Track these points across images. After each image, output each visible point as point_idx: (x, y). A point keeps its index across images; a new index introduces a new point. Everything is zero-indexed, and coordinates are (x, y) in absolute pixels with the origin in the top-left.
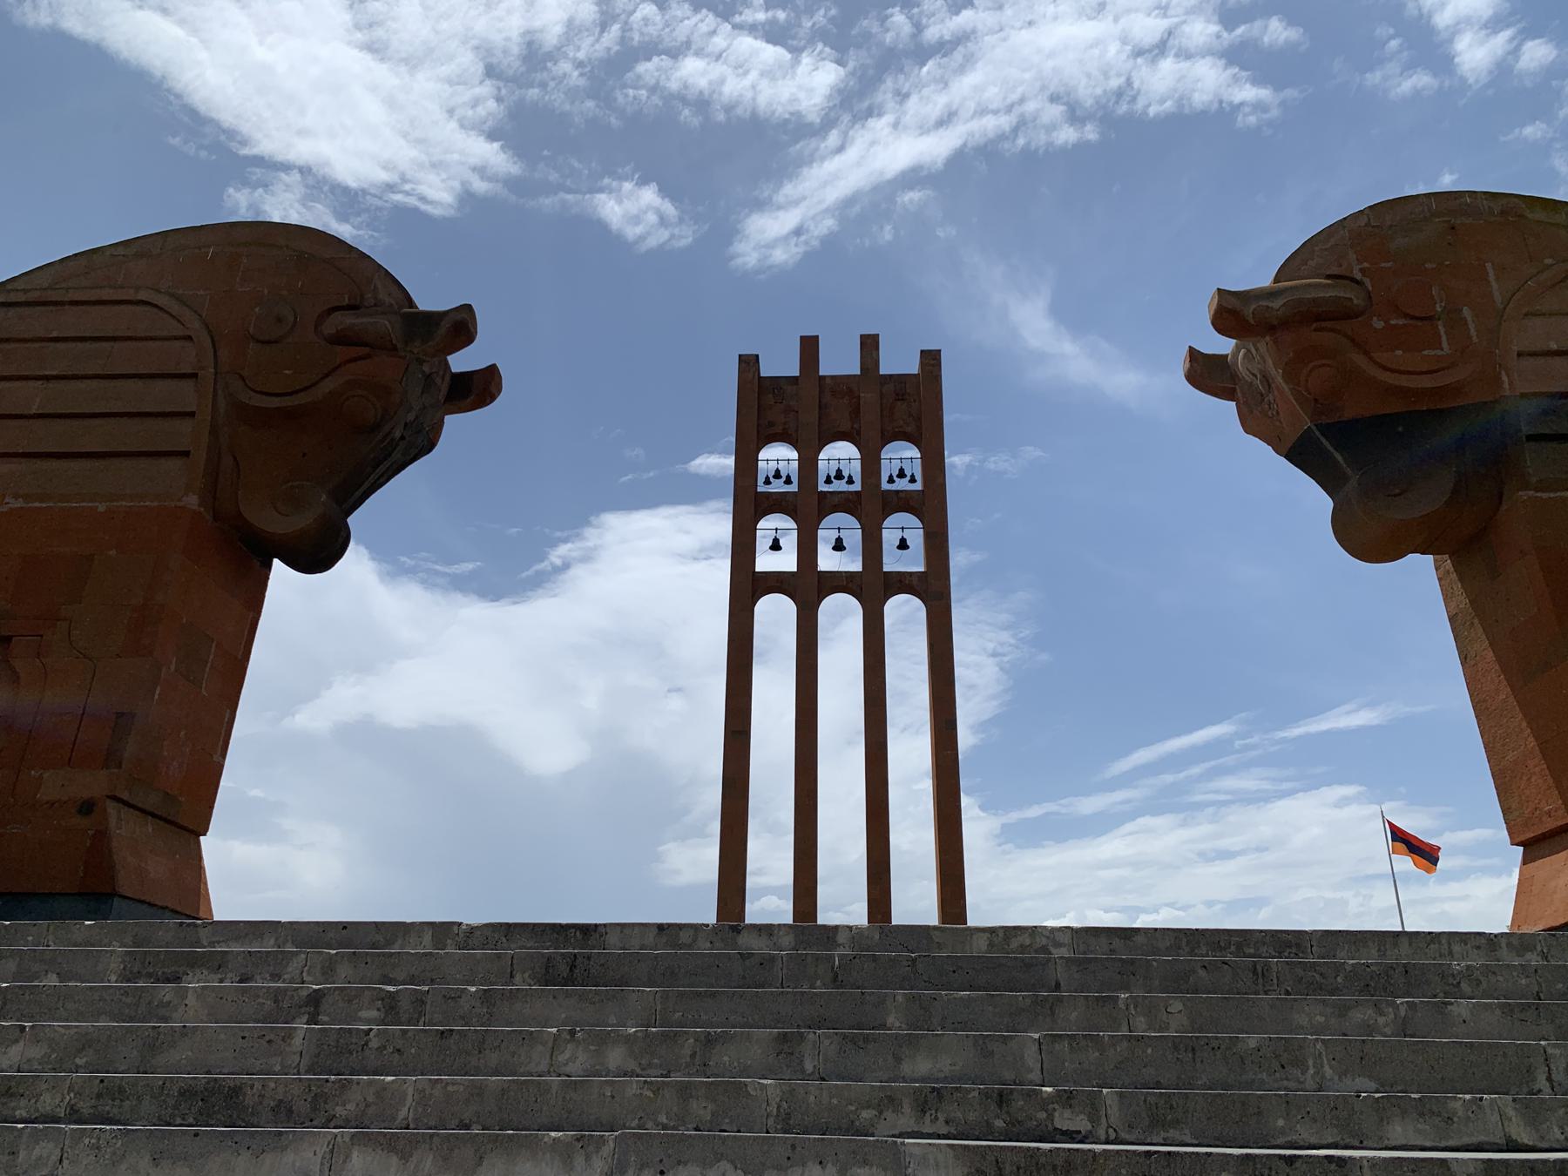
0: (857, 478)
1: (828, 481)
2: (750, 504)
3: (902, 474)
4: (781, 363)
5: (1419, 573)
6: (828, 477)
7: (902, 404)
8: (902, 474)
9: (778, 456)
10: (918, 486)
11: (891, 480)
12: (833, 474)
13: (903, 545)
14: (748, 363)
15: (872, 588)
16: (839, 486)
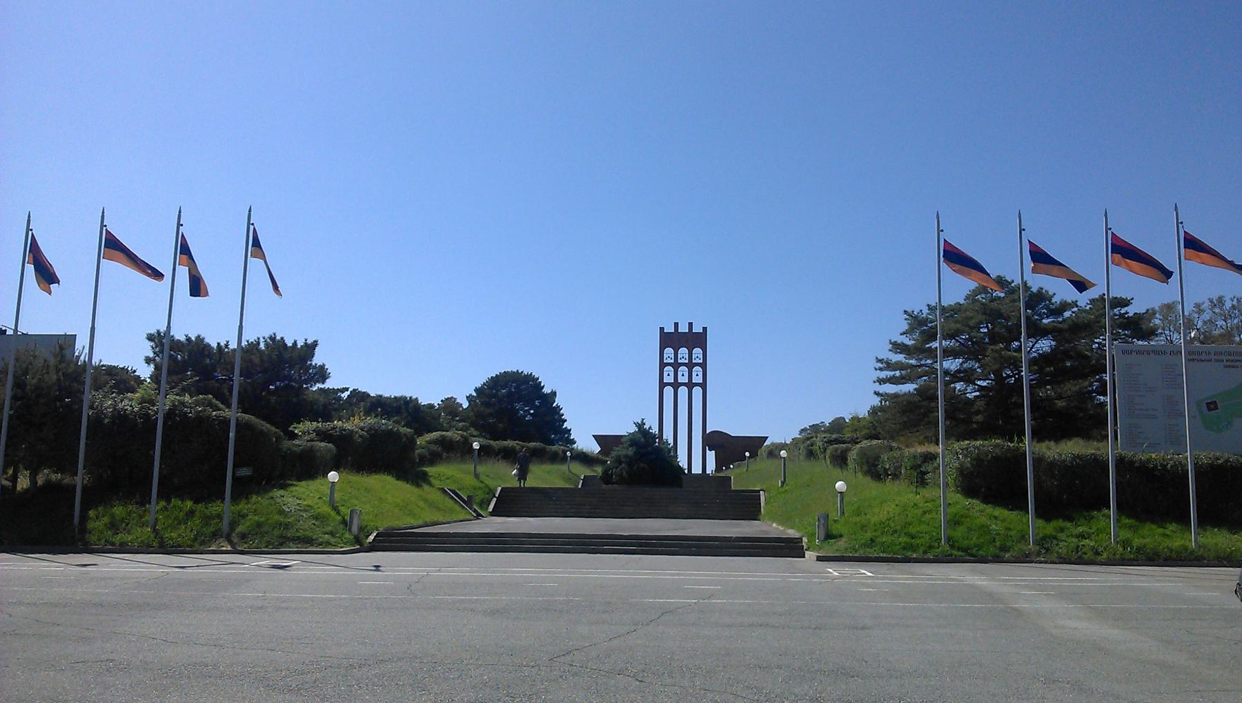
2: (663, 365)
4: (670, 329)
7: (697, 340)
9: (669, 351)
14: (662, 329)
15: (690, 385)
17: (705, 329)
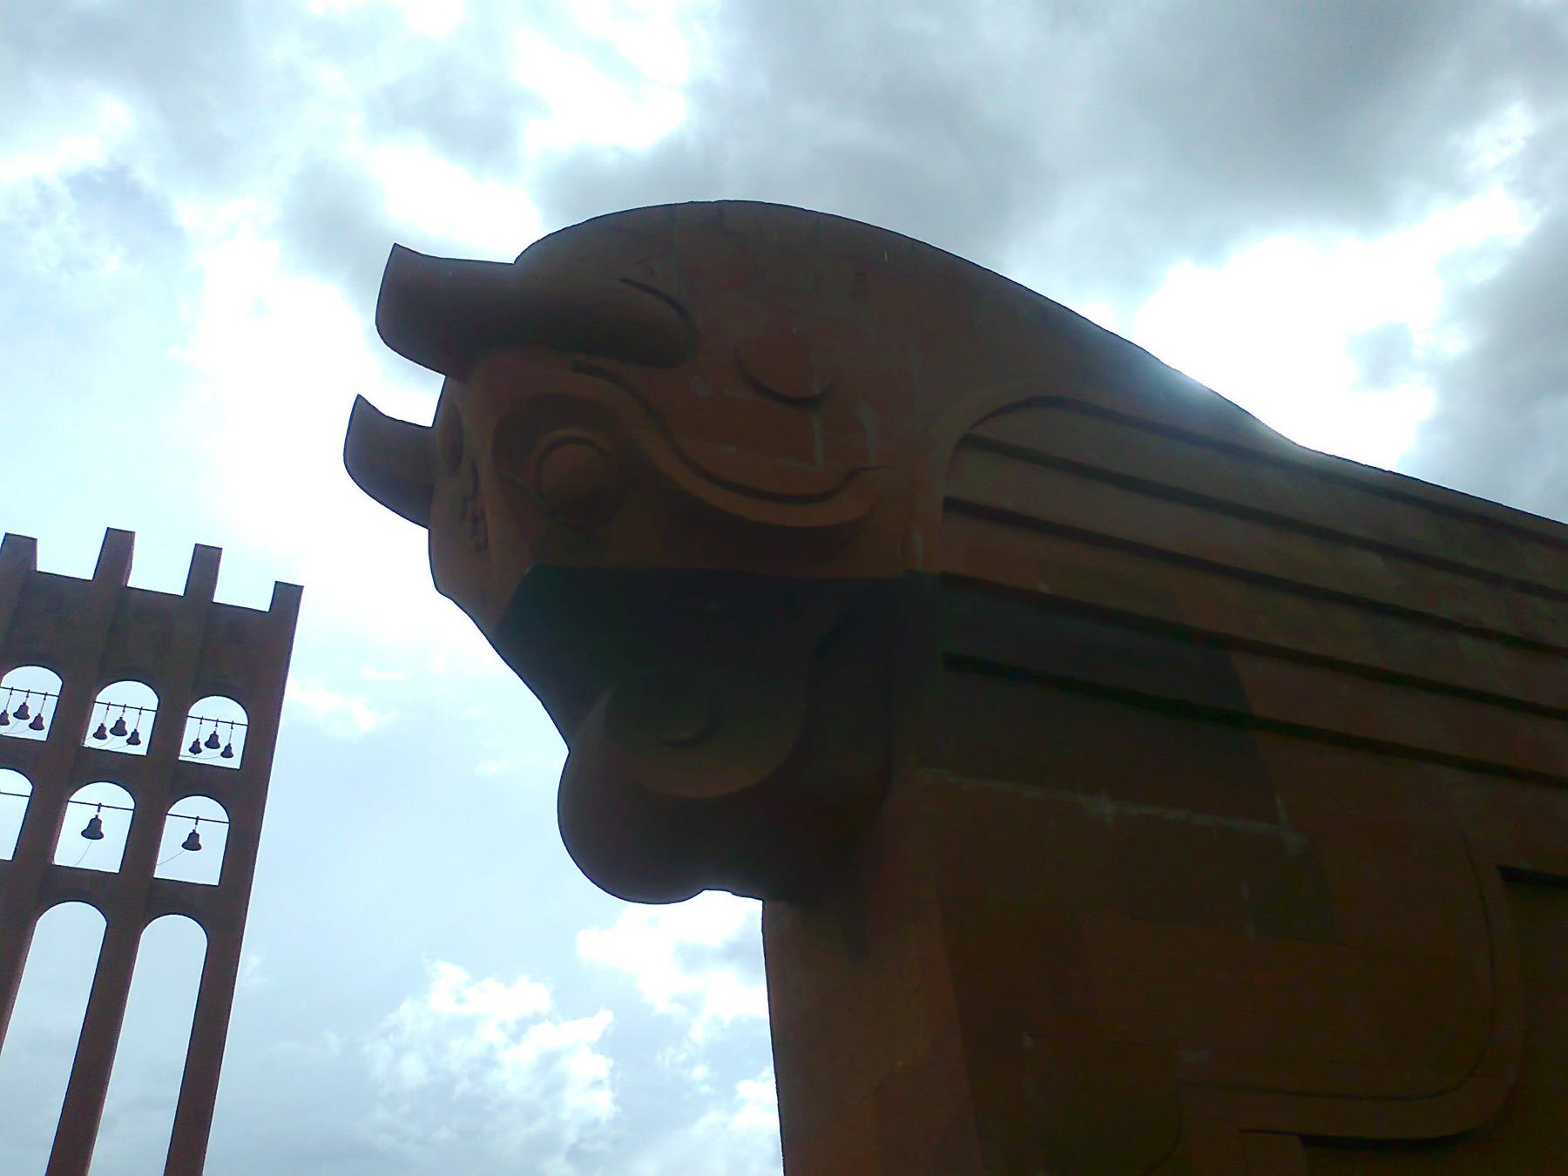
0: (145, 737)
1: (100, 734)
3: (213, 742)
5: (727, 920)
6: (102, 728)
8: (213, 742)
10: (234, 763)
11: (195, 749)
12: (110, 725)
13: (192, 843)
16: (116, 744)
17: (287, 597)
